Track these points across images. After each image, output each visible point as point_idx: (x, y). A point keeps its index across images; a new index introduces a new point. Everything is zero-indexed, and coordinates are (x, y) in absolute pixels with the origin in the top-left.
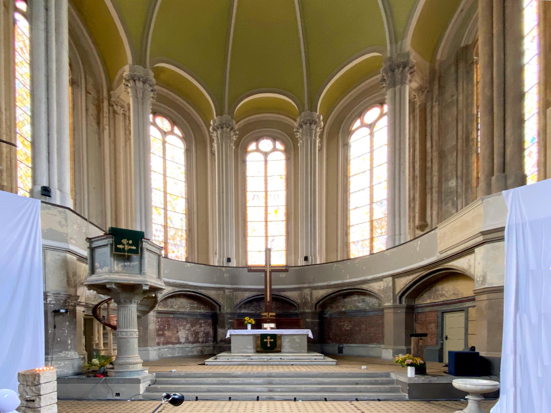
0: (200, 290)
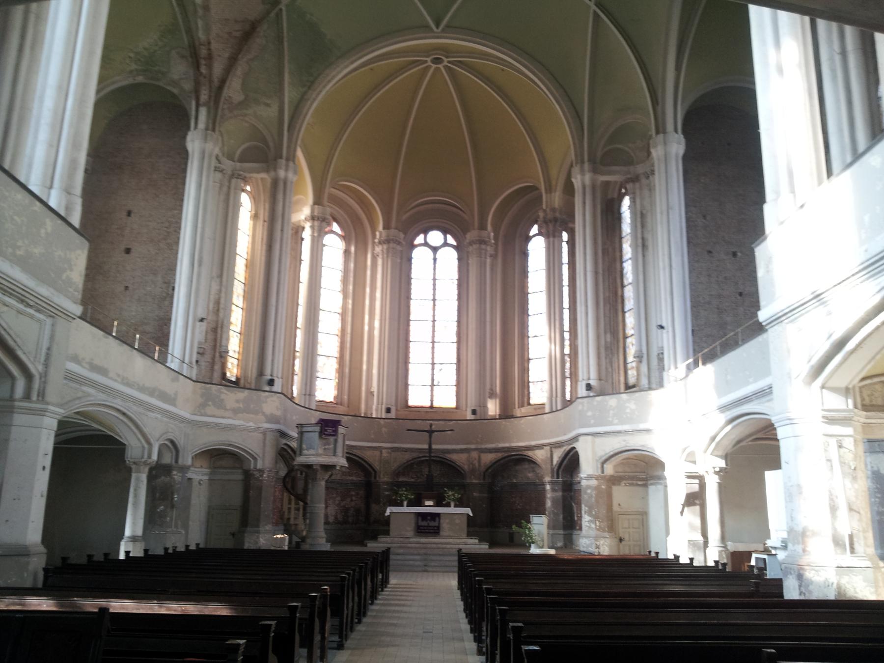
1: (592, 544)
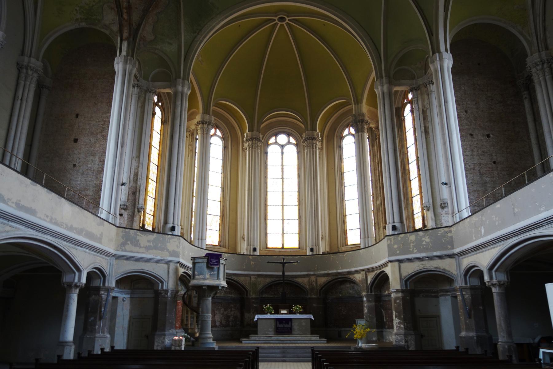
0: (233, 277)
1: (402, 339)
